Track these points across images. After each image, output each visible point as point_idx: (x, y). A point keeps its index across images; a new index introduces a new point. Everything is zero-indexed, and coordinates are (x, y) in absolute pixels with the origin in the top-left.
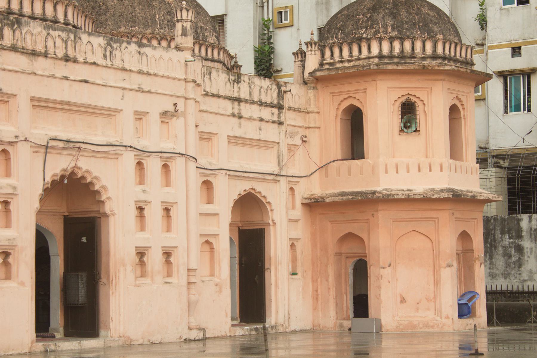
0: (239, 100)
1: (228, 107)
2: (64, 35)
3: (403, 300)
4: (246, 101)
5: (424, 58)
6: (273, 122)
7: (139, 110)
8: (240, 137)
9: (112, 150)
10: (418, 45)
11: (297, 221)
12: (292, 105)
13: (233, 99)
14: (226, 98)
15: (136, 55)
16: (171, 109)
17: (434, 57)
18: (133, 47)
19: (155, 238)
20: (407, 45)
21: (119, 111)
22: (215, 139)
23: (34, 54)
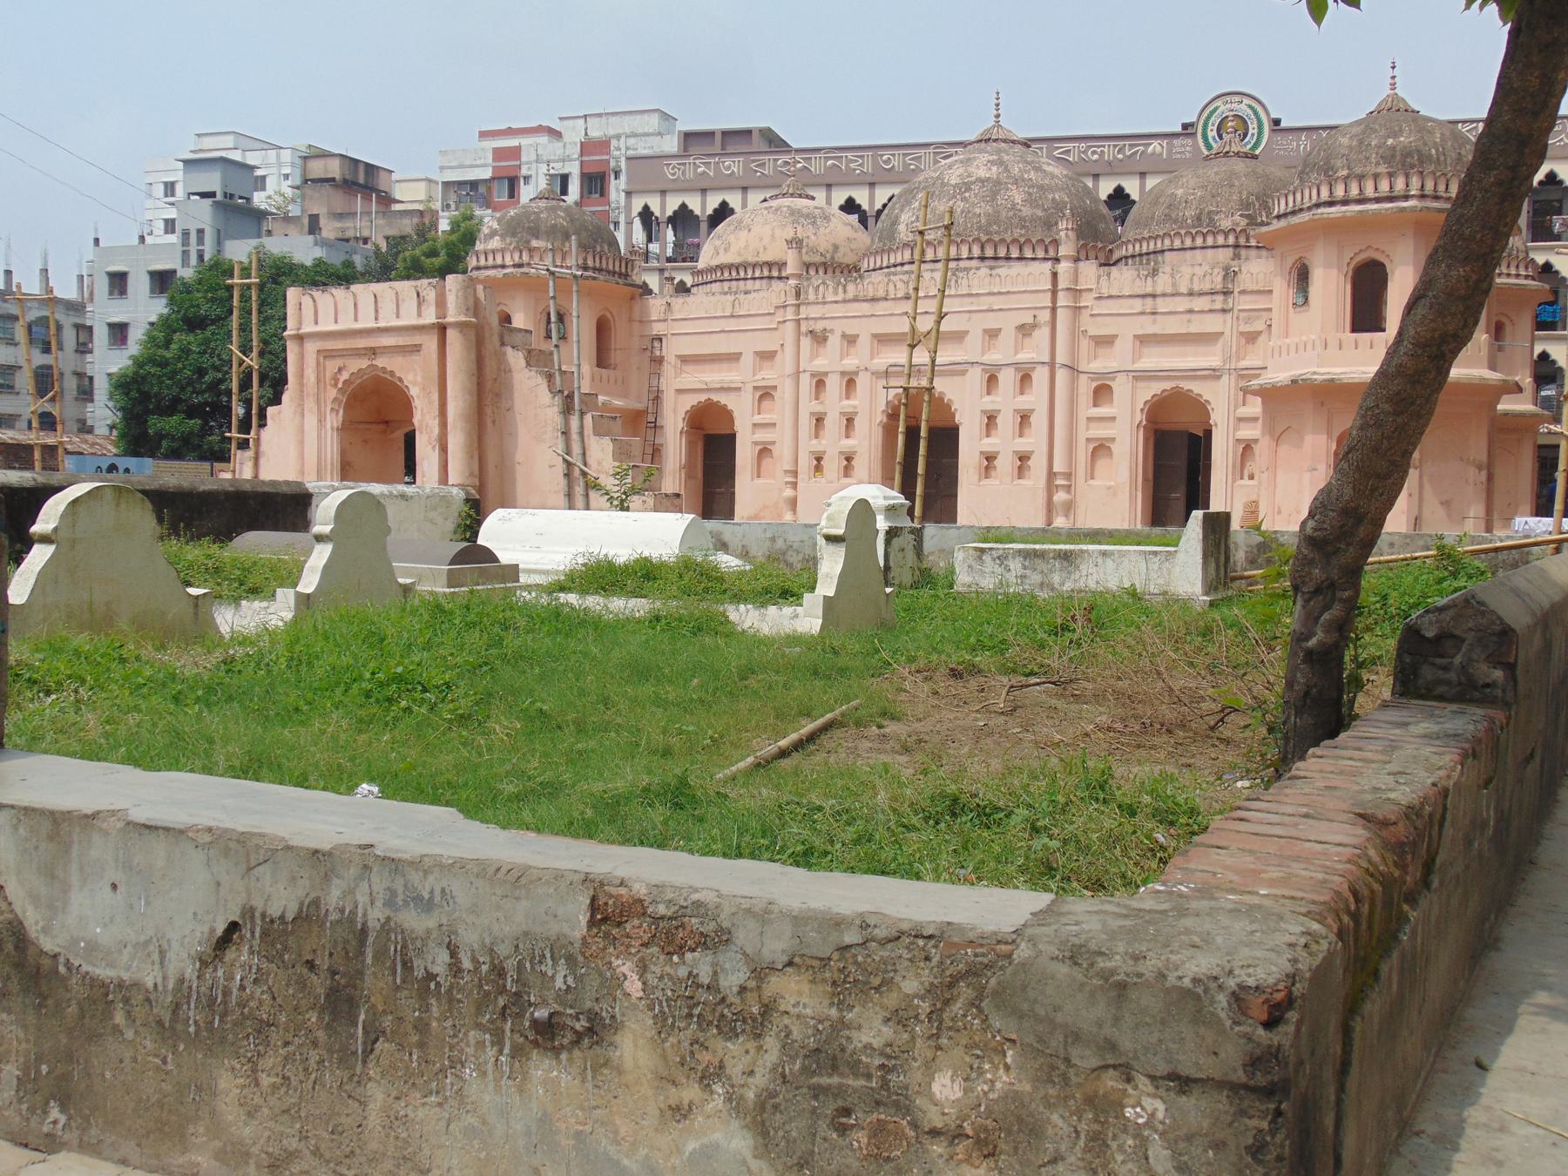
0: (1154, 296)
1: (1138, 305)
2: (905, 278)
4: (1164, 295)
5: (1309, 209)
8: (1155, 335)
9: (957, 369)
10: (1307, 192)
11: (1255, 419)
12: (1250, 287)
13: (1144, 296)
14: (1131, 296)
15: (987, 279)
16: (1030, 320)
17: (1318, 205)
18: (984, 271)
19: (1004, 442)
22: (1117, 342)
23: (874, 300)
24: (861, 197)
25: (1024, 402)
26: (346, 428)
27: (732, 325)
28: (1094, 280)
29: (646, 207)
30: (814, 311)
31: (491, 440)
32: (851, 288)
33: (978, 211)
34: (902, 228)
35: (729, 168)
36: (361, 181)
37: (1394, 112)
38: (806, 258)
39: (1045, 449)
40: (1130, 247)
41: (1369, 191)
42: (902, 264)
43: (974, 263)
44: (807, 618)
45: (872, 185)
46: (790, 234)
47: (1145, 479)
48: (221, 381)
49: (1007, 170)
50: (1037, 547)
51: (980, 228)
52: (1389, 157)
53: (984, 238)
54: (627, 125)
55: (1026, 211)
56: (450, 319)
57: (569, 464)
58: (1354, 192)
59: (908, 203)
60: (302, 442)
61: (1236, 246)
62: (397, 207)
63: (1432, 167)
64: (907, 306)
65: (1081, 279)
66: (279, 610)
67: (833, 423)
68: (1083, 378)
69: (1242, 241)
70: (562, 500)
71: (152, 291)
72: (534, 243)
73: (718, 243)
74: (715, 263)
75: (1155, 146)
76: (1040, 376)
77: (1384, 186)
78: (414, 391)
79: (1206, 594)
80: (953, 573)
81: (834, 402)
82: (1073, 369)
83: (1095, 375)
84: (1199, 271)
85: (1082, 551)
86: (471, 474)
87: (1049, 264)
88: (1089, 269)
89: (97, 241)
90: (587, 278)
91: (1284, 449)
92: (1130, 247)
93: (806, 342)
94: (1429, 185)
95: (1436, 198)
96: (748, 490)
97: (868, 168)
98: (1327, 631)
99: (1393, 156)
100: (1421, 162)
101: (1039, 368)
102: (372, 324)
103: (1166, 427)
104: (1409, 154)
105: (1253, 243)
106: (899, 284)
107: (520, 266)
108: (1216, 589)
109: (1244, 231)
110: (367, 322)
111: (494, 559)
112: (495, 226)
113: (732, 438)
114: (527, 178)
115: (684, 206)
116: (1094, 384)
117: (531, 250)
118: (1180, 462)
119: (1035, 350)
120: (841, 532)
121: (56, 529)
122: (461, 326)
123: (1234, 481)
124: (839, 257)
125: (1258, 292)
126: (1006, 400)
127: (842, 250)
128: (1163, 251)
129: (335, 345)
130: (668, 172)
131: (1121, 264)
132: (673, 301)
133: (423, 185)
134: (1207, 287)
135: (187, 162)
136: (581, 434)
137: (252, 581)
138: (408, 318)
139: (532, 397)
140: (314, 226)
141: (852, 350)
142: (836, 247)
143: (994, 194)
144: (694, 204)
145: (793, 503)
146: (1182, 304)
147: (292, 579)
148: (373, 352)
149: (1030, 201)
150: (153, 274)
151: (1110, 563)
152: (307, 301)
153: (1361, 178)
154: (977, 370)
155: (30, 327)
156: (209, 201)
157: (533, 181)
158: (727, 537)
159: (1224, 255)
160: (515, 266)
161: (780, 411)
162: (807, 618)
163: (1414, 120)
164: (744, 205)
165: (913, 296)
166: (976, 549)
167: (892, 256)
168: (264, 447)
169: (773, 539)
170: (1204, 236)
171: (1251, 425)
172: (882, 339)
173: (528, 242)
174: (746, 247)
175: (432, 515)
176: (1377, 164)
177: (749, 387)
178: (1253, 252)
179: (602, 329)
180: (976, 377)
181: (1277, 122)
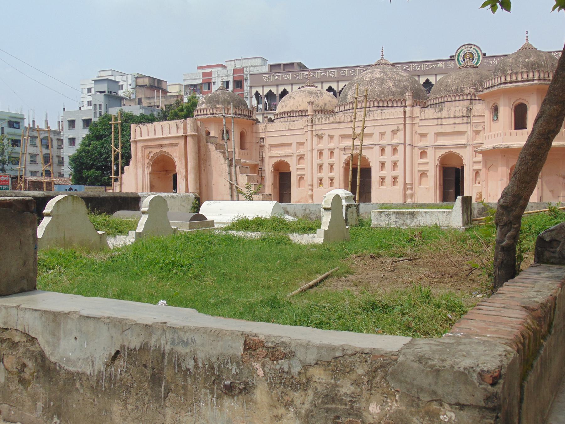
0: (441, 118)
1: (435, 122)
2: (350, 114)
3: (490, 196)
4: (445, 118)
5: (498, 85)
6: (462, 123)
7: (381, 131)
9: (370, 147)
10: (496, 79)
11: (480, 162)
12: (476, 114)
13: (438, 119)
16: (396, 129)
17: (501, 84)
18: (379, 111)
19: (388, 172)
20: (493, 81)
21: (373, 133)
22: (428, 135)
23: (340, 122)
24: (334, 86)
25: (395, 158)
26: (152, 173)
27: (289, 133)
28: (419, 113)
29: (257, 92)
30: (318, 127)
31: (203, 176)
32: (331, 118)
33: (376, 90)
34: (349, 96)
35: (286, 77)
36: (156, 86)
37: (528, 49)
38: (315, 108)
39: (403, 175)
40: (432, 101)
41: (520, 78)
42: (349, 110)
43: (375, 108)
44: (318, 238)
45: (338, 81)
46: (309, 100)
47: (440, 185)
48: (108, 158)
49: (386, 75)
50: (401, 210)
51: (377, 96)
52: (526, 66)
53: (379, 99)
54: (249, 63)
55: (394, 89)
56: (188, 134)
57: (231, 184)
58: (514, 79)
59: (351, 88)
60: (137, 179)
61: (471, 100)
62: (169, 94)
63: (543, 69)
64: (352, 125)
65: (414, 113)
66: (130, 239)
67: (326, 167)
68: (416, 149)
69: (473, 98)
70: (229, 197)
71: (84, 127)
72: (218, 106)
73: (283, 104)
74: (282, 111)
75: (440, 65)
76: (400, 149)
77: (525, 76)
78: (176, 160)
79: (464, 226)
80: (371, 220)
81: (326, 160)
82: (412, 146)
83: (420, 148)
84: (458, 109)
85: (417, 212)
86: (197, 189)
87: (403, 108)
88: (417, 109)
89: (64, 109)
90: (236, 118)
91: (491, 173)
92: (432, 101)
93: (315, 139)
94: (542, 76)
95: (545, 80)
96: (296, 192)
97: (336, 75)
98: (509, 240)
99: (528, 65)
100: (538, 67)
101: (400, 146)
102: (160, 136)
103: (448, 166)
104: (534, 64)
105: (477, 98)
106: (349, 117)
107: (213, 114)
108: (467, 224)
109: (473, 94)
110: (159, 136)
111: (206, 219)
112: (204, 100)
113: (289, 174)
114: (214, 83)
115: (270, 91)
116: (420, 151)
117: (216, 108)
118: (453, 178)
119: (398, 139)
120: (329, 206)
121: (52, 211)
122: (192, 136)
123: (473, 185)
124: (327, 108)
125: (480, 116)
126: (388, 157)
127: (327, 105)
128: (444, 102)
129: (148, 144)
130: (264, 79)
131: (429, 107)
132: (267, 125)
133: (178, 86)
134: (460, 114)
135: (95, 81)
136: (236, 173)
137: (120, 228)
138: (174, 134)
139: (218, 162)
140: (140, 102)
141: (332, 141)
142: (325, 104)
143: (382, 83)
144: (274, 90)
145: (312, 196)
146: (451, 121)
147: (134, 227)
148: (161, 146)
149: (395, 85)
150: (84, 120)
151: (428, 216)
152: (138, 128)
153: (516, 74)
154: (378, 147)
155: (41, 140)
156: (103, 94)
157: (216, 84)
158: (288, 209)
159: (467, 103)
160: (211, 114)
161: (306, 163)
162: (318, 238)
163: (536, 52)
164: (292, 90)
165: (354, 121)
166: (379, 212)
167: (346, 107)
168: (123, 181)
169: (305, 210)
170: (459, 96)
171: (478, 164)
172: (343, 137)
173: (215, 105)
174: (293, 105)
175: (183, 203)
176: (522, 68)
177: (295, 155)
178: (477, 102)
179: (242, 136)
180: (377, 149)
181: (485, 54)
